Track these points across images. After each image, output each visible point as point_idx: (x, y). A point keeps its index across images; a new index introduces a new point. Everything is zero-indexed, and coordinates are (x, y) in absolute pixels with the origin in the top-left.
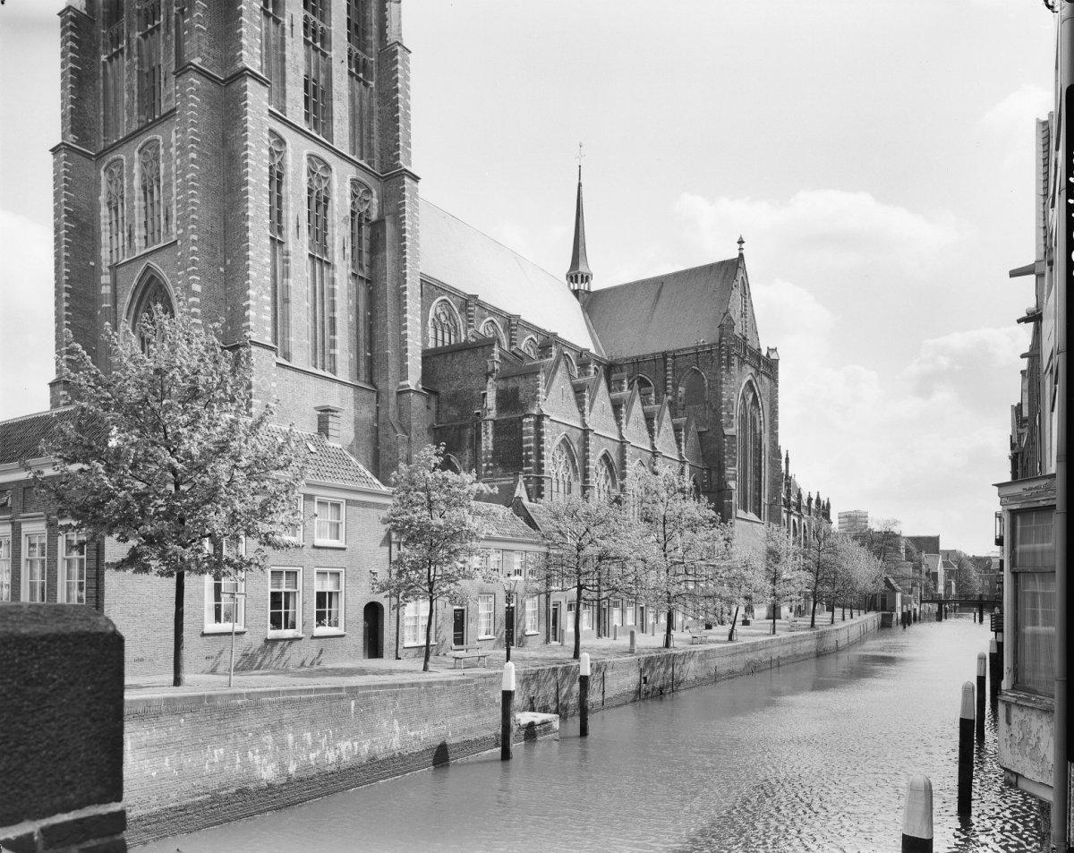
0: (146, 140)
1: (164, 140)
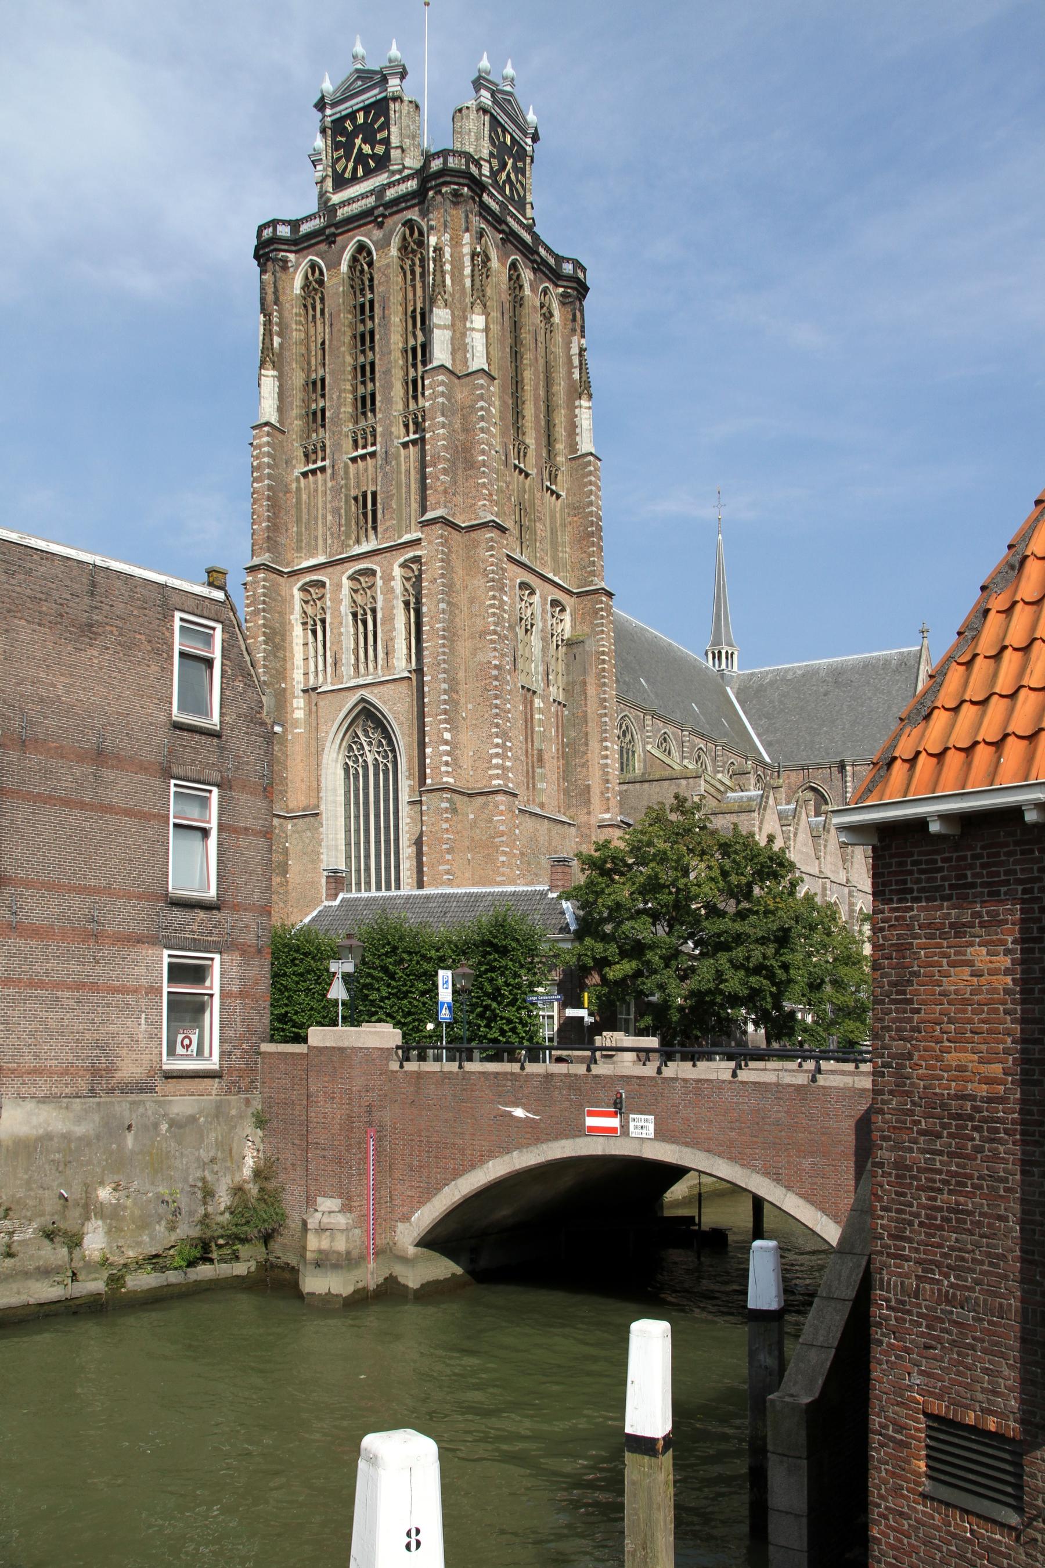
1: (383, 572)
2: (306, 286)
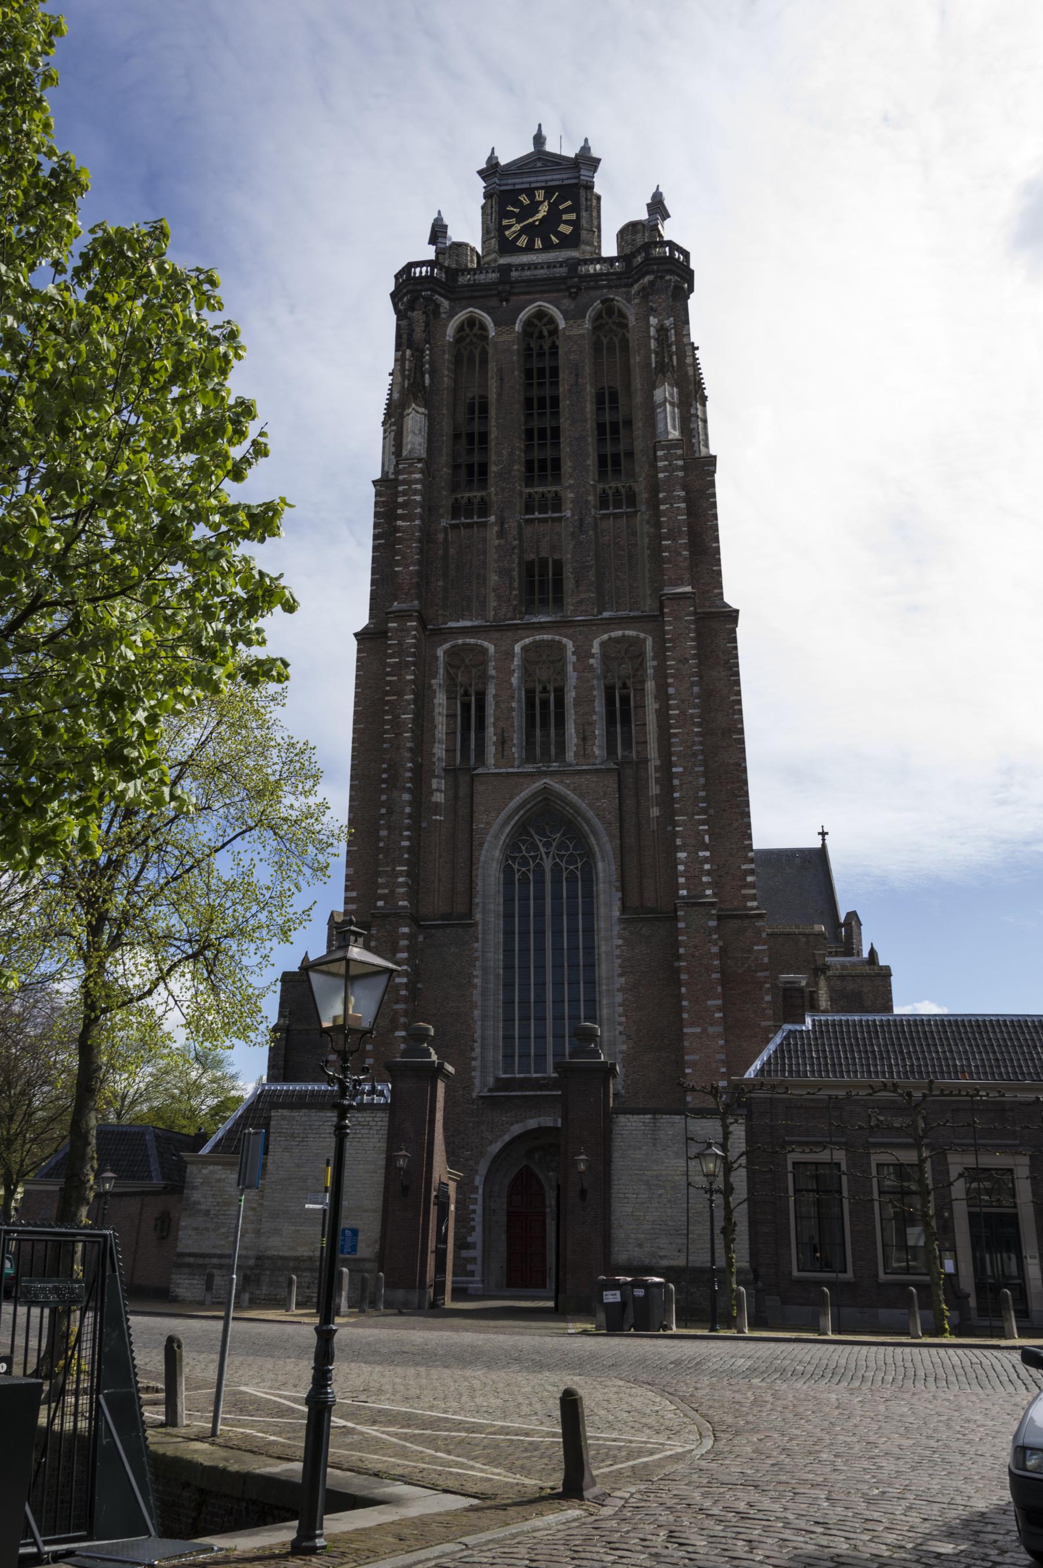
0: (537, 638)
2: (458, 340)
